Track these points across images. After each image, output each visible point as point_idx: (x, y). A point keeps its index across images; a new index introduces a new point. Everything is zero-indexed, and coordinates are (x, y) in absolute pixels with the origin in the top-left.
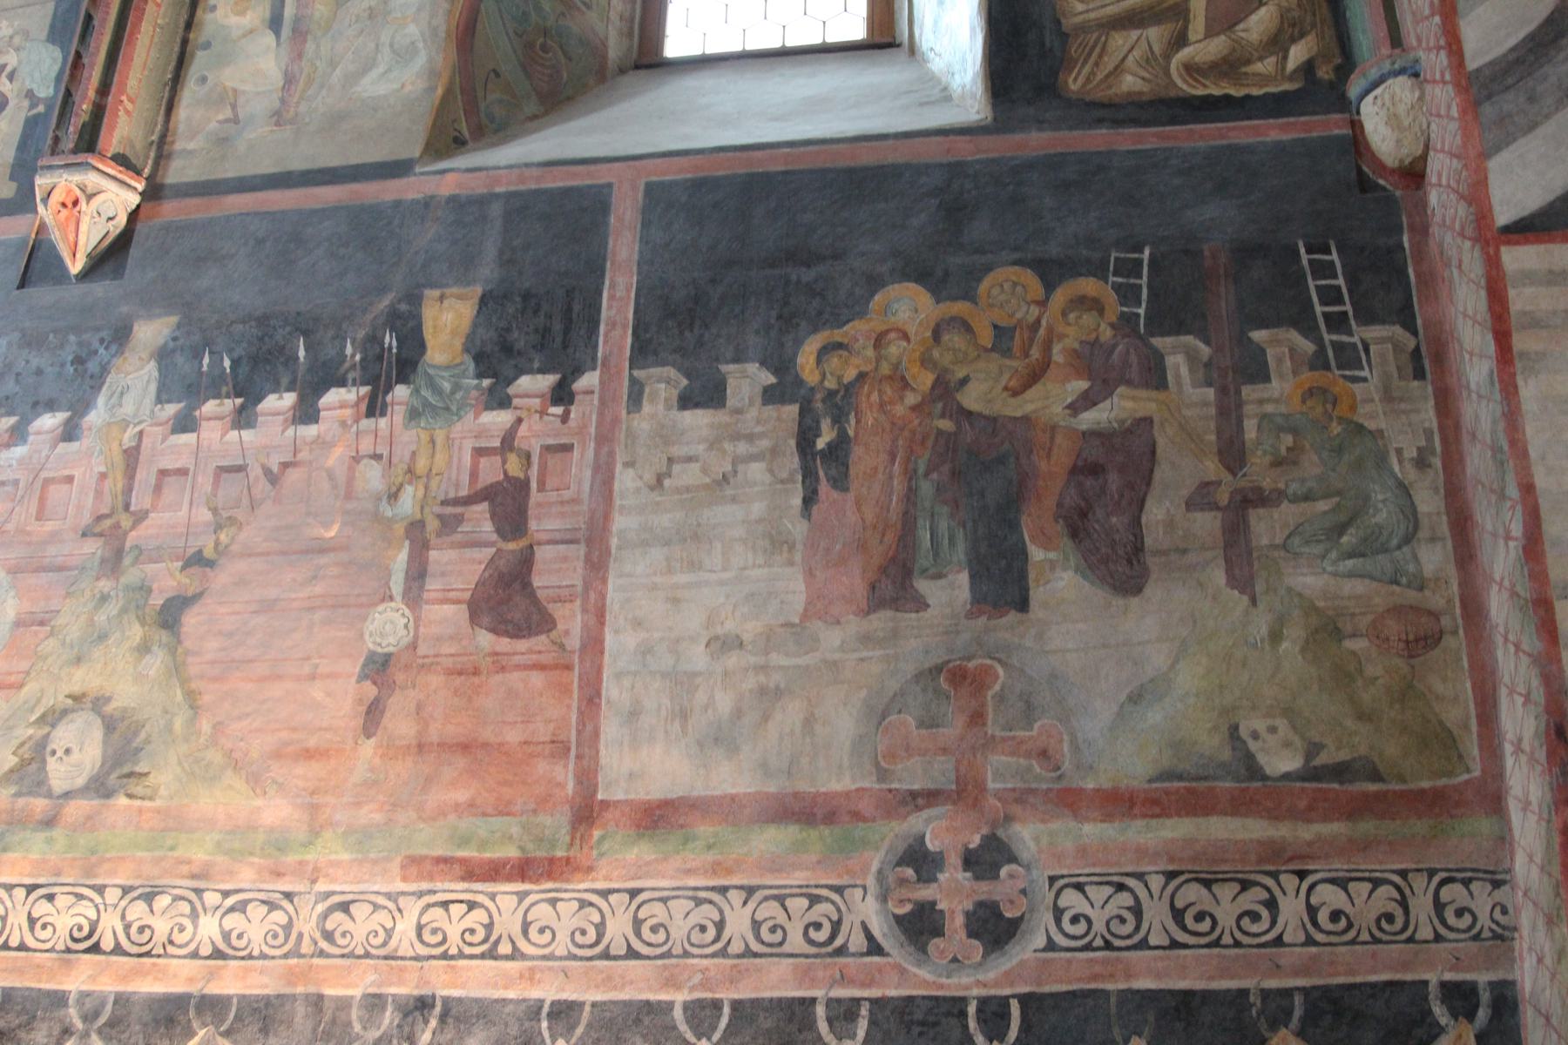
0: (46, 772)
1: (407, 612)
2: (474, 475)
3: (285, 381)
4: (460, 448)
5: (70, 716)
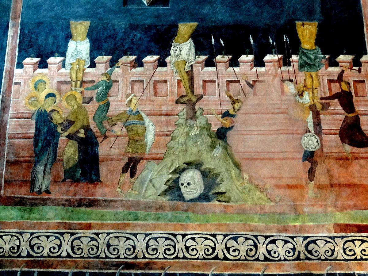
0: (181, 192)
1: (317, 137)
2: (330, 89)
3: (247, 50)
4: (323, 79)
5: (187, 170)
